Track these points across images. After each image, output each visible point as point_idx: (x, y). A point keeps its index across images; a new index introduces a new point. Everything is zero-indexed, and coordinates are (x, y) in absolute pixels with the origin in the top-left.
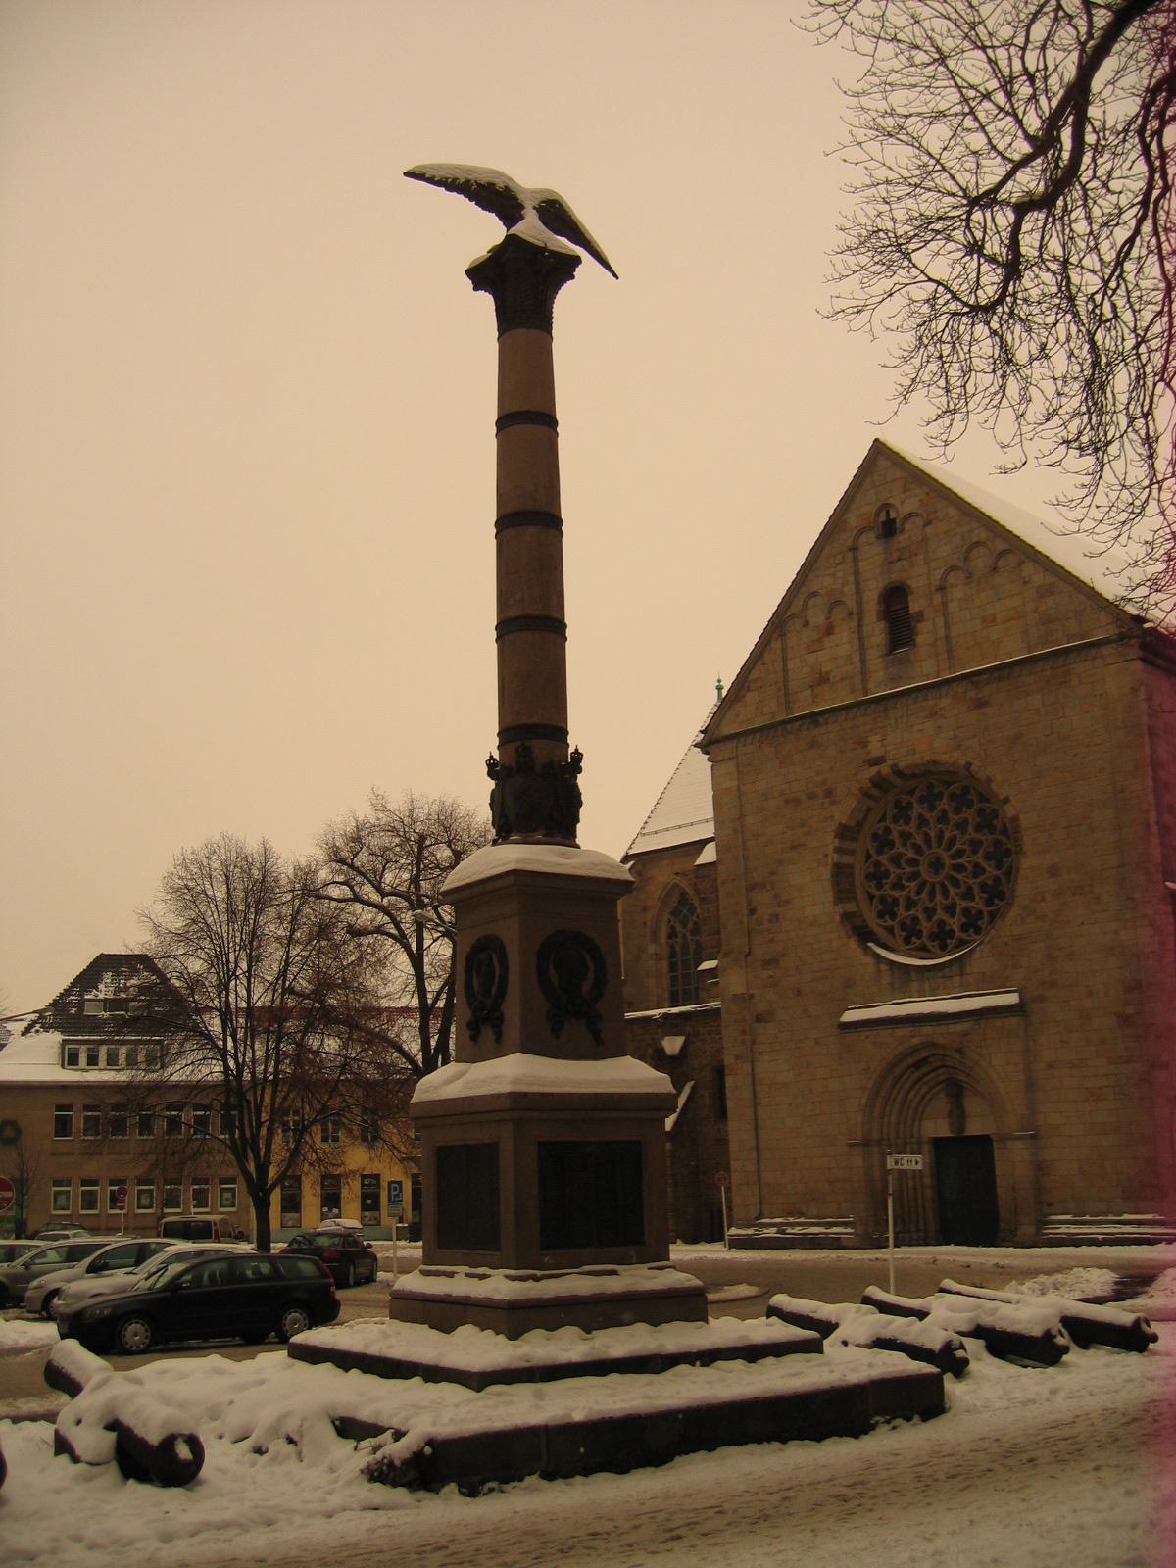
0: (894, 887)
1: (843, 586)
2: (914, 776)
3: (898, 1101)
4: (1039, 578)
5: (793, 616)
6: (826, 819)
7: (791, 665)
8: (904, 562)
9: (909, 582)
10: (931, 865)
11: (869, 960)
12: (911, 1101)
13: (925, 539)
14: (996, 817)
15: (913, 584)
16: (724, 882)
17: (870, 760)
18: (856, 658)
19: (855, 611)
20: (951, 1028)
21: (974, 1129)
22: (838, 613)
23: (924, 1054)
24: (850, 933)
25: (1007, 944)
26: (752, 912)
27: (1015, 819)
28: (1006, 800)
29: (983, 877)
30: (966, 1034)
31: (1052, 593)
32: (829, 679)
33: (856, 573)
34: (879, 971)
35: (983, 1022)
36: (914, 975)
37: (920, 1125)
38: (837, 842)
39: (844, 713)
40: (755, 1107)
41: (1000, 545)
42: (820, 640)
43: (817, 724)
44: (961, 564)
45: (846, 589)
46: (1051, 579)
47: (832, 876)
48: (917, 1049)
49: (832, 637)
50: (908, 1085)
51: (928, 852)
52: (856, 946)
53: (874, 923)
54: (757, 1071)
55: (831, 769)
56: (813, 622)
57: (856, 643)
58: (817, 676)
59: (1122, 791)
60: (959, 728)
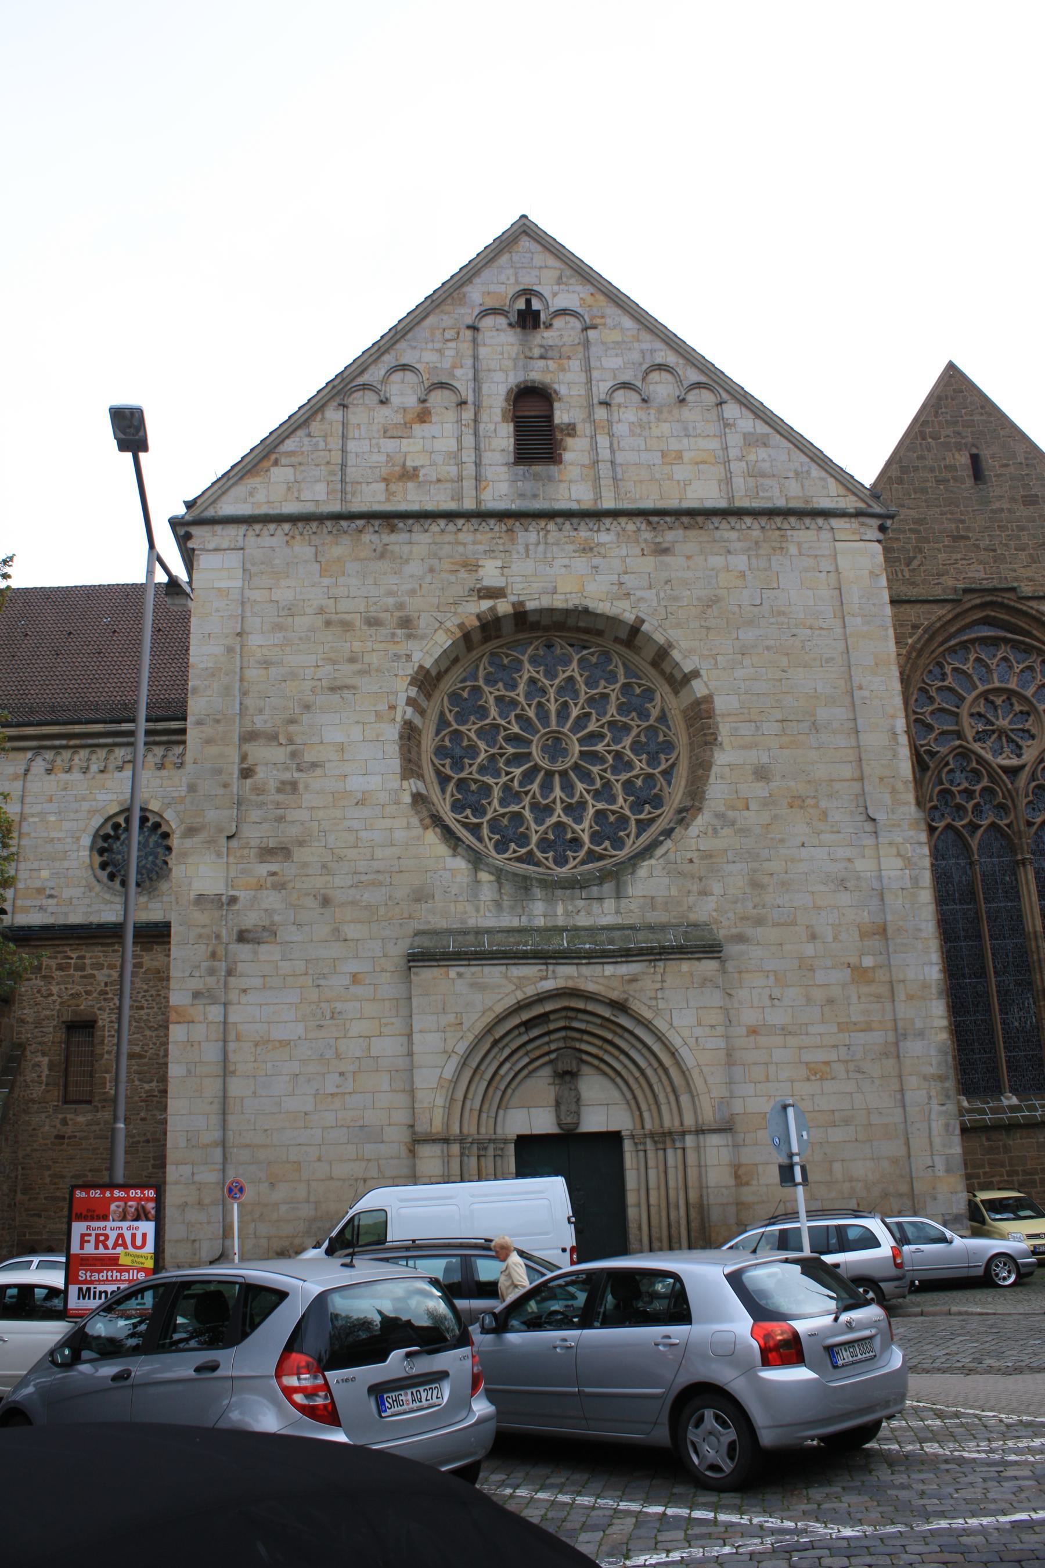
0: (482, 770)
1: (454, 367)
2: (535, 626)
3: (488, 1076)
4: (747, 423)
5: (365, 387)
6: (397, 656)
7: (351, 446)
8: (550, 362)
9: (556, 386)
10: (545, 749)
11: (460, 864)
12: (503, 1077)
13: (586, 344)
14: (652, 700)
15: (563, 390)
16: (199, 723)
17: (479, 590)
18: (469, 456)
19: (470, 399)
20: (609, 970)
21: (593, 1121)
22: (437, 398)
23: (549, 1007)
24: (428, 821)
25: (691, 861)
26: (246, 773)
27: (708, 699)
28: (695, 674)
29: (630, 774)
30: (633, 980)
31: (765, 445)
32: (417, 476)
33: (475, 357)
34: (477, 882)
35: (661, 964)
36: (537, 892)
37: (504, 1116)
38: (413, 692)
39: (442, 522)
40: (225, 1076)
41: (694, 376)
42: (407, 425)
43: (393, 530)
44: (639, 384)
45: (458, 372)
46: (762, 428)
47: (401, 737)
48: (542, 998)
49: (425, 426)
50: (507, 1052)
51: (543, 731)
52: (437, 841)
53: (449, 817)
54: (232, 1019)
55: (412, 593)
56: (395, 400)
57: (469, 441)
58: (397, 469)
59: (860, 688)
60: (626, 573)
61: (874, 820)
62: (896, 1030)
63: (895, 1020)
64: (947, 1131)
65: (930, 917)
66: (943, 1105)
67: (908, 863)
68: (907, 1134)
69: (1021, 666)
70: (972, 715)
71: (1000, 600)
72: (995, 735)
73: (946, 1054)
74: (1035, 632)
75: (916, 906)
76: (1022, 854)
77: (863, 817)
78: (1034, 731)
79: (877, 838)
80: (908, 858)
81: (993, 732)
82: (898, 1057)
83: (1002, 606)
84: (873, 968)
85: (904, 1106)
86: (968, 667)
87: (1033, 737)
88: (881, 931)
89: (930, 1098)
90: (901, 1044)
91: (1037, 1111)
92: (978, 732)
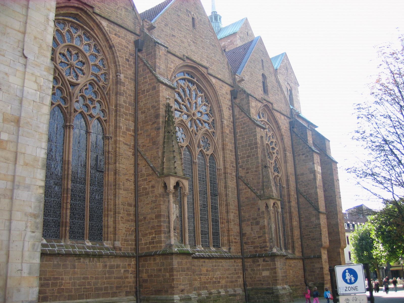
61: (26, 57)
62: (13, 181)
63: (14, 176)
64: (33, 248)
65: (45, 122)
66: (33, 232)
67: (40, 88)
68: (9, 248)
69: (86, 42)
70: (60, 54)
71: (85, 9)
72: (69, 67)
73: (40, 202)
74: (95, 30)
75: (40, 113)
76: (70, 123)
77: (20, 54)
78: (85, 71)
79: (25, 68)
80: (41, 86)
81: (68, 65)
82: (12, 198)
83: (86, 12)
84: (7, 141)
85: (10, 230)
86: (64, 32)
87: (84, 74)
88: (16, 121)
89: (27, 227)
90: (15, 191)
91: (56, 248)
92: (61, 62)
